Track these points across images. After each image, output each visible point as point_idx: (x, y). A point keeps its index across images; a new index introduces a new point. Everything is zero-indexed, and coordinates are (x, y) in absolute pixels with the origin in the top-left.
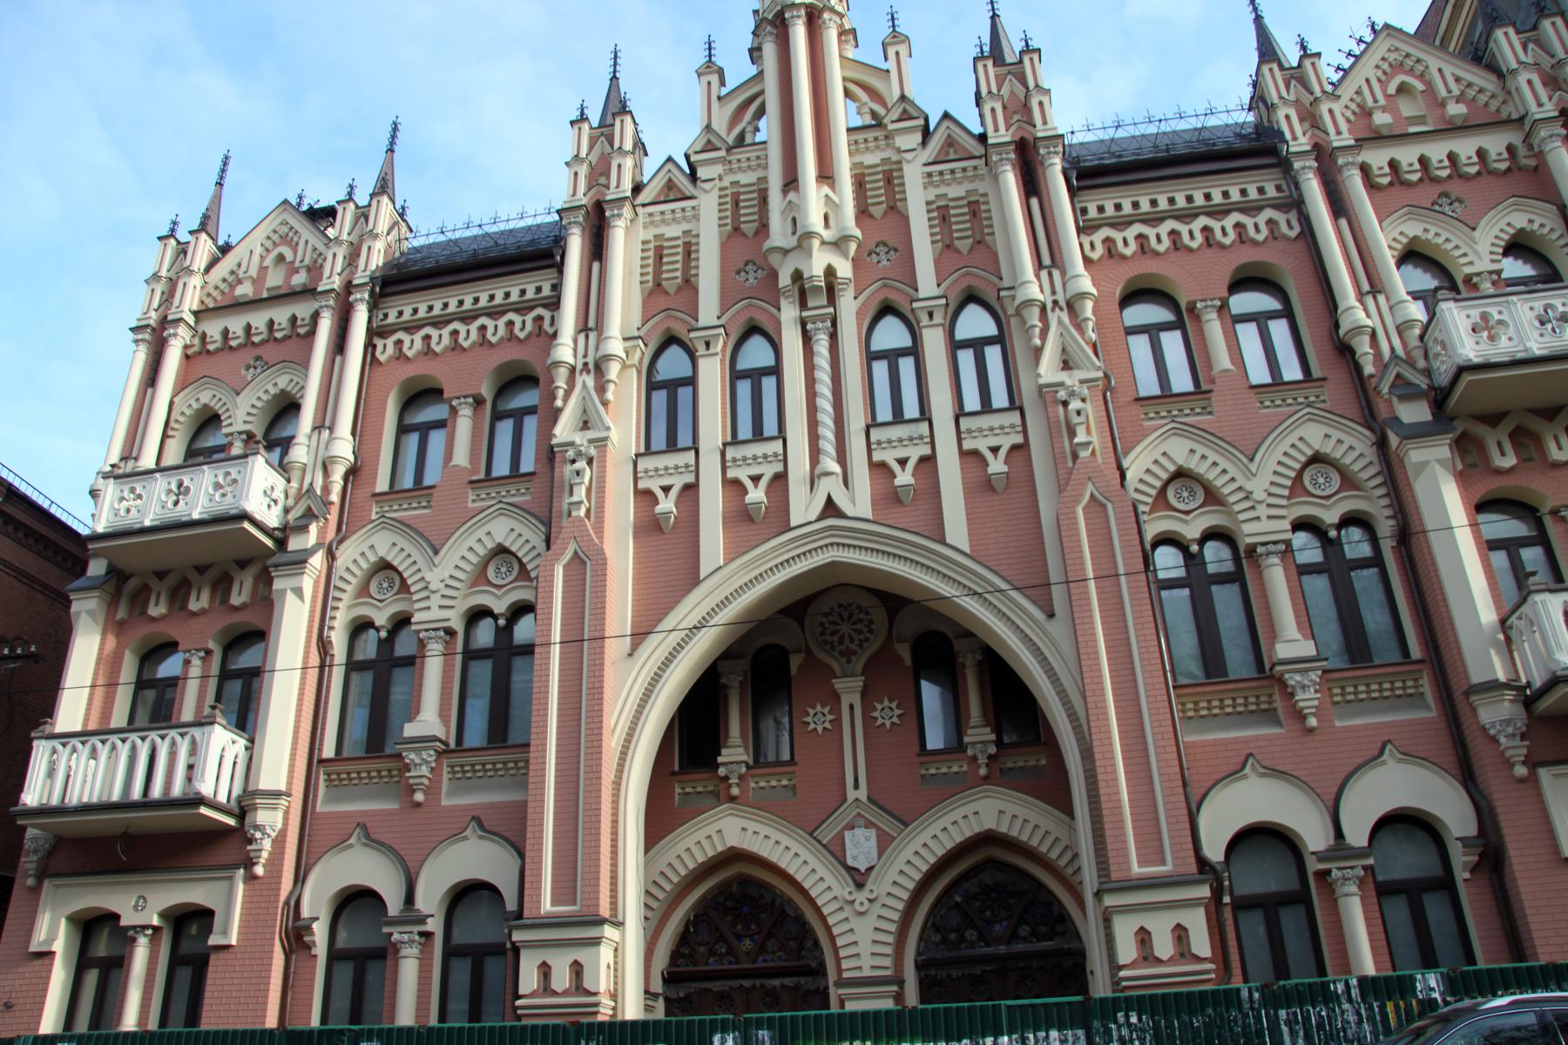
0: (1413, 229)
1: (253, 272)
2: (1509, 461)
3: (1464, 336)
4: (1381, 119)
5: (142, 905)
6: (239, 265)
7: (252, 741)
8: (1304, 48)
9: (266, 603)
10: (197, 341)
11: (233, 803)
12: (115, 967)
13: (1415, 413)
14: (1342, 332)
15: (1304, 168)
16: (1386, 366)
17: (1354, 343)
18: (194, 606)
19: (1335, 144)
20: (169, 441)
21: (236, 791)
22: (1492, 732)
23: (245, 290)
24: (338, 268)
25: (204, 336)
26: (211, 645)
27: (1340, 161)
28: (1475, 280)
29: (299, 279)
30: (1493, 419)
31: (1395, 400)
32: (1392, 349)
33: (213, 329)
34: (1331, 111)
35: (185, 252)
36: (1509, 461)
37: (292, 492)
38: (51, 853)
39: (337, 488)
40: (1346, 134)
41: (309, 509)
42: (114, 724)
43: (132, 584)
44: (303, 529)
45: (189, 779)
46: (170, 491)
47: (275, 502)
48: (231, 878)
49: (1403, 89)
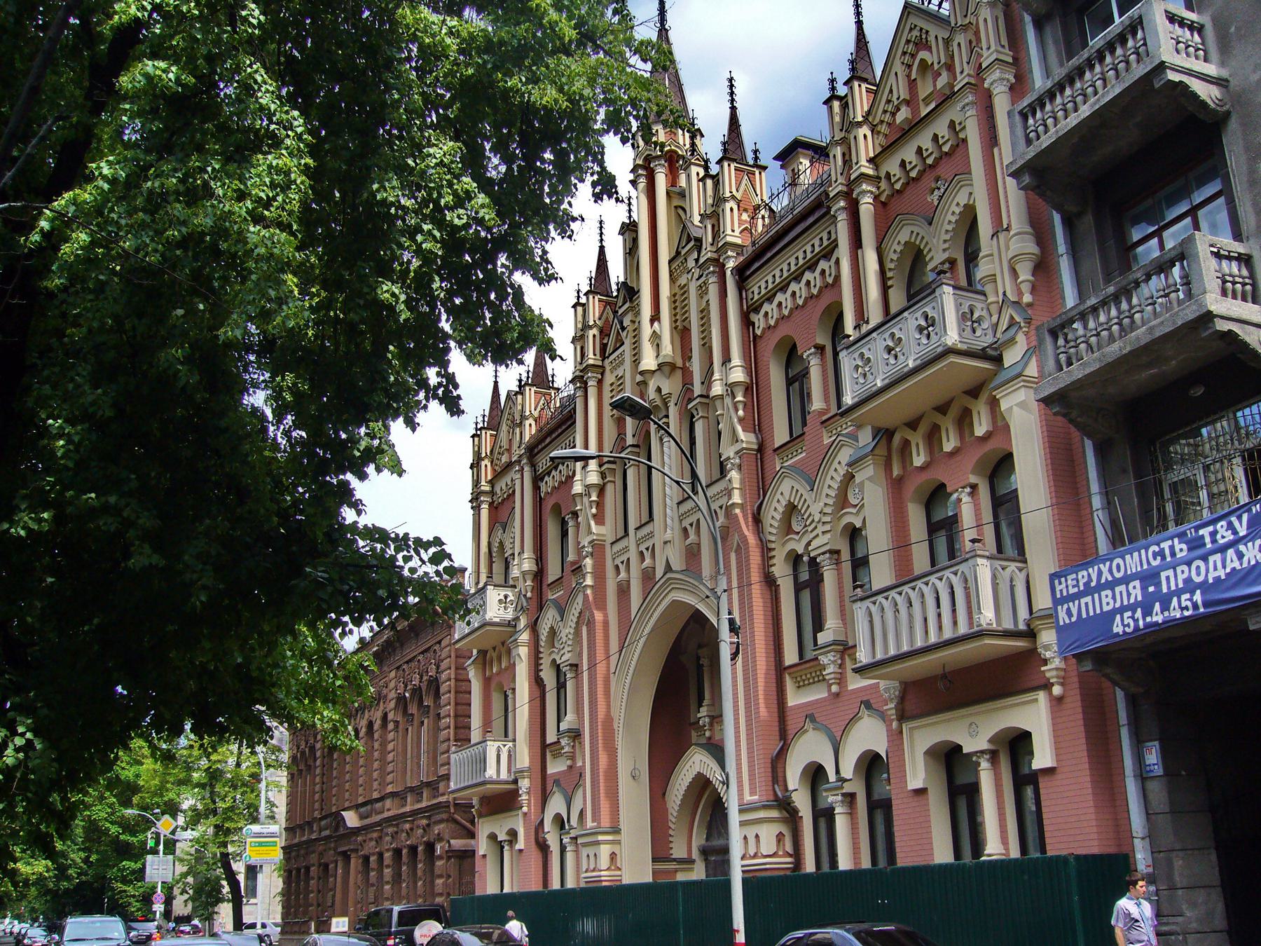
1: (904, 94)
5: (974, 733)
6: (891, 91)
7: (1025, 562)
9: (1001, 427)
10: (883, 185)
11: (1022, 627)
12: (973, 791)
18: (948, 447)
20: (891, 291)
21: (1023, 614)
23: (903, 114)
24: (965, 60)
25: (888, 175)
26: (973, 479)
29: (942, 81)
33: (892, 166)
35: (847, 103)
37: (994, 309)
38: (902, 699)
39: (1025, 288)
41: (1012, 318)
42: (917, 572)
43: (897, 439)
44: (1012, 341)
45: (970, 617)
46: (857, 367)
47: (979, 321)
48: (1036, 700)
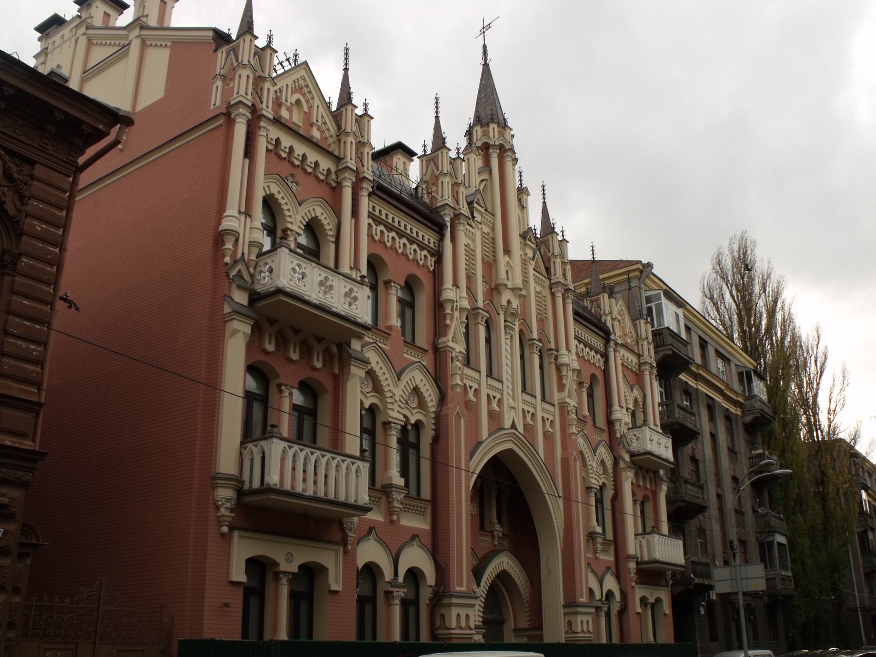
0: (274, 189)
2: (271, 348)
3: (290, 273)
4: (284, 114)
8: (270, 42)
13: (241, 298)
14: (221, 228)
15: (244, 115)
16: (236, 262)
17: (226, 238)
19: (264, 112)
22: (220, 503)
27: (262, 124)
28: (289, 232)
30: (272, 322)
31: (234, 286)
32: (243, 254)
34: (269, 89)
36: (271, 348)
40: (270, 110)
49: (298, 102)
